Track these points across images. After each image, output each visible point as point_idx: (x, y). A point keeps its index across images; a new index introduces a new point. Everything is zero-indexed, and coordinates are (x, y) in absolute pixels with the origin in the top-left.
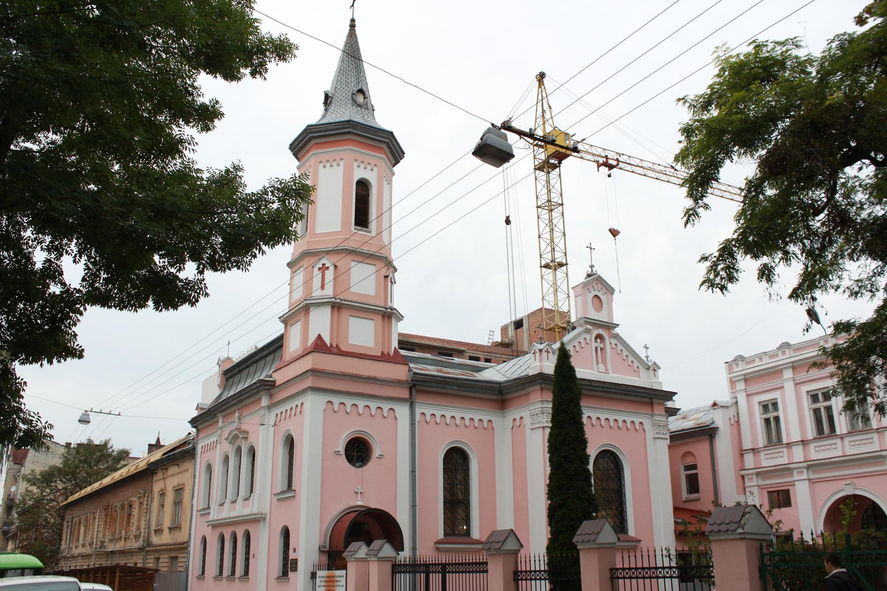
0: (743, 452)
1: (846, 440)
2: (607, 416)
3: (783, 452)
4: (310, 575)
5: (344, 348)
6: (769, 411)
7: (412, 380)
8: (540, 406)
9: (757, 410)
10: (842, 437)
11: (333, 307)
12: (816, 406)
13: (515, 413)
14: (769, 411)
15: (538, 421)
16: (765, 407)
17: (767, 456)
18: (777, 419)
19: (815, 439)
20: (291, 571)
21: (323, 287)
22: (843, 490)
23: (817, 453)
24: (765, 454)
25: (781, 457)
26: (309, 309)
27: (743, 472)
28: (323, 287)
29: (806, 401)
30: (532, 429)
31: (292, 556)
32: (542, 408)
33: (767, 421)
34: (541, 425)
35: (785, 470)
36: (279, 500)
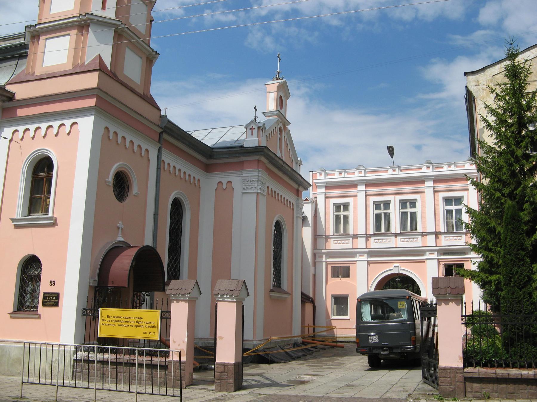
0: (316, 237)
1: (399, 238)
2: (282, 194)
3: (349, 240)
4: (81, 312)
5: (121, 78)
6: (340, 211)
7: (165, 127)
8: (257, 174)
9: (331, 208)
10: (396, 235)
11: (115, 32)
12: (378, 212)
13: (223, 177)
14: (340, 211)
15: (252, 186)
16: (338, 207)
17: (336, 242)
18: (346, 218)
19: (374, 235)
20: (44, 304)
21: (103, 7)
22: (392, 270)
23: (375, 243)
24: (334, 240)
25: (347, 243)
26: (88, 26)
27: (316, 251)
28: (103, 7)
29: (371, 207)
30: (243, 193)
31: (44, 287)
32: (258, 176)
33: (338, 218)
34: (256, 191)
35: (351, 254)
36: (16, 226)
